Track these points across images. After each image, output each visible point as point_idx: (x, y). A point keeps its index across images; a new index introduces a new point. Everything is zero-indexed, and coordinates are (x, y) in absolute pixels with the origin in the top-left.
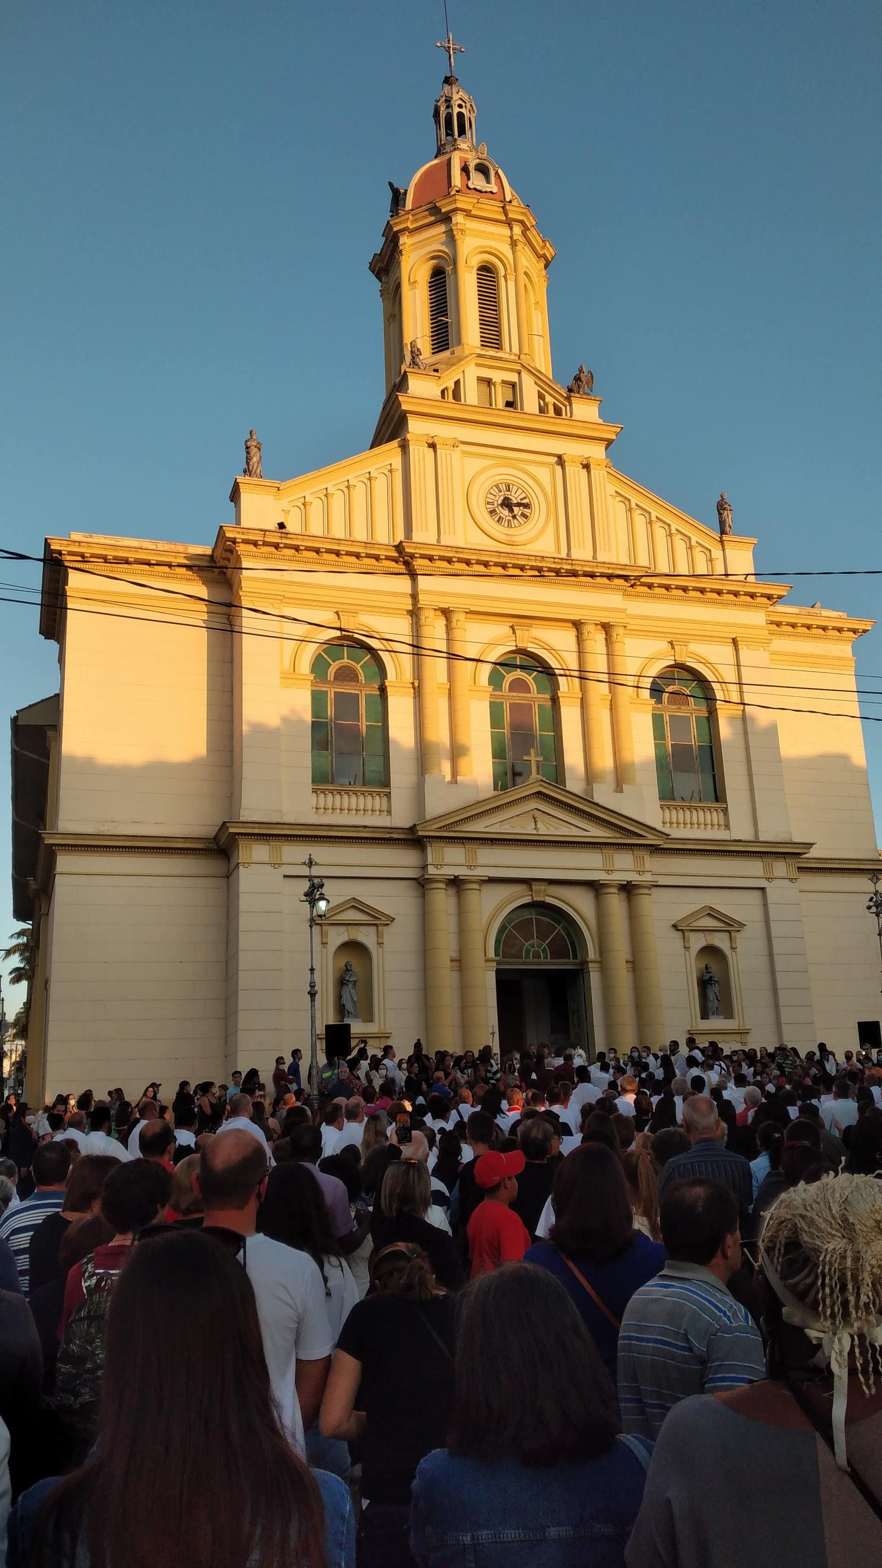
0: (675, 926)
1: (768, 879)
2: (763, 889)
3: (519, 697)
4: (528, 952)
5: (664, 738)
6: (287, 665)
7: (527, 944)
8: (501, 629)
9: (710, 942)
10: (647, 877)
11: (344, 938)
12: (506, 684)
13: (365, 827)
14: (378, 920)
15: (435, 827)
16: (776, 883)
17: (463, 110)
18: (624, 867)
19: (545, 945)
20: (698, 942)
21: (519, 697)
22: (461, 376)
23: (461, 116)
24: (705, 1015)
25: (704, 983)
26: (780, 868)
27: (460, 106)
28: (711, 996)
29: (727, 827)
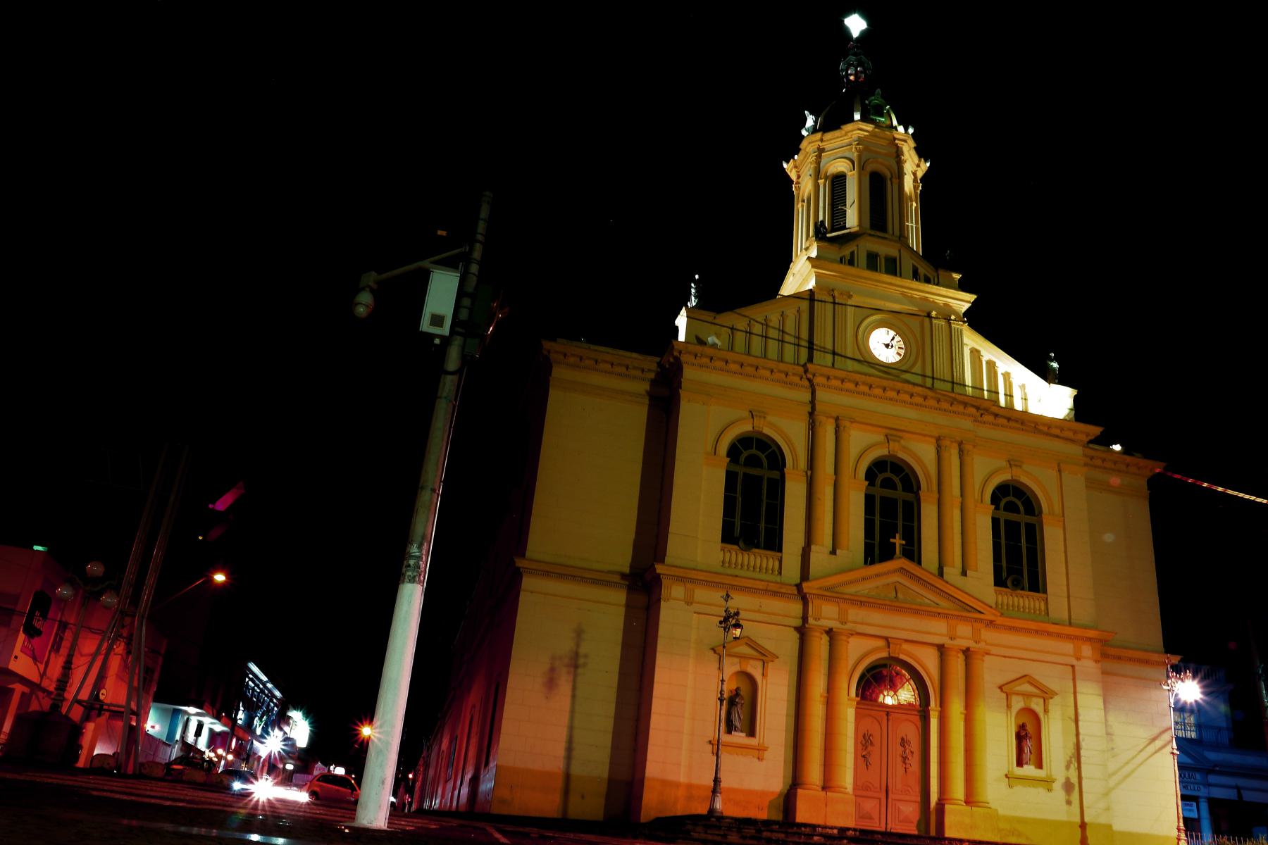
0: (1001, 688)
1: (1078, 659)
2: (1073, 666)
3: (888, 493)
6: (709, 448)
10: (982, 645)
11: (737, 668)
12: (878, 482)
14: (765, 657)
18: (964, 635)
20: (1018, 703)
21: (888, 493)
22: (855, 248)
24: (1020, 763)
25: (1021, 737)
28: (1027, 750)
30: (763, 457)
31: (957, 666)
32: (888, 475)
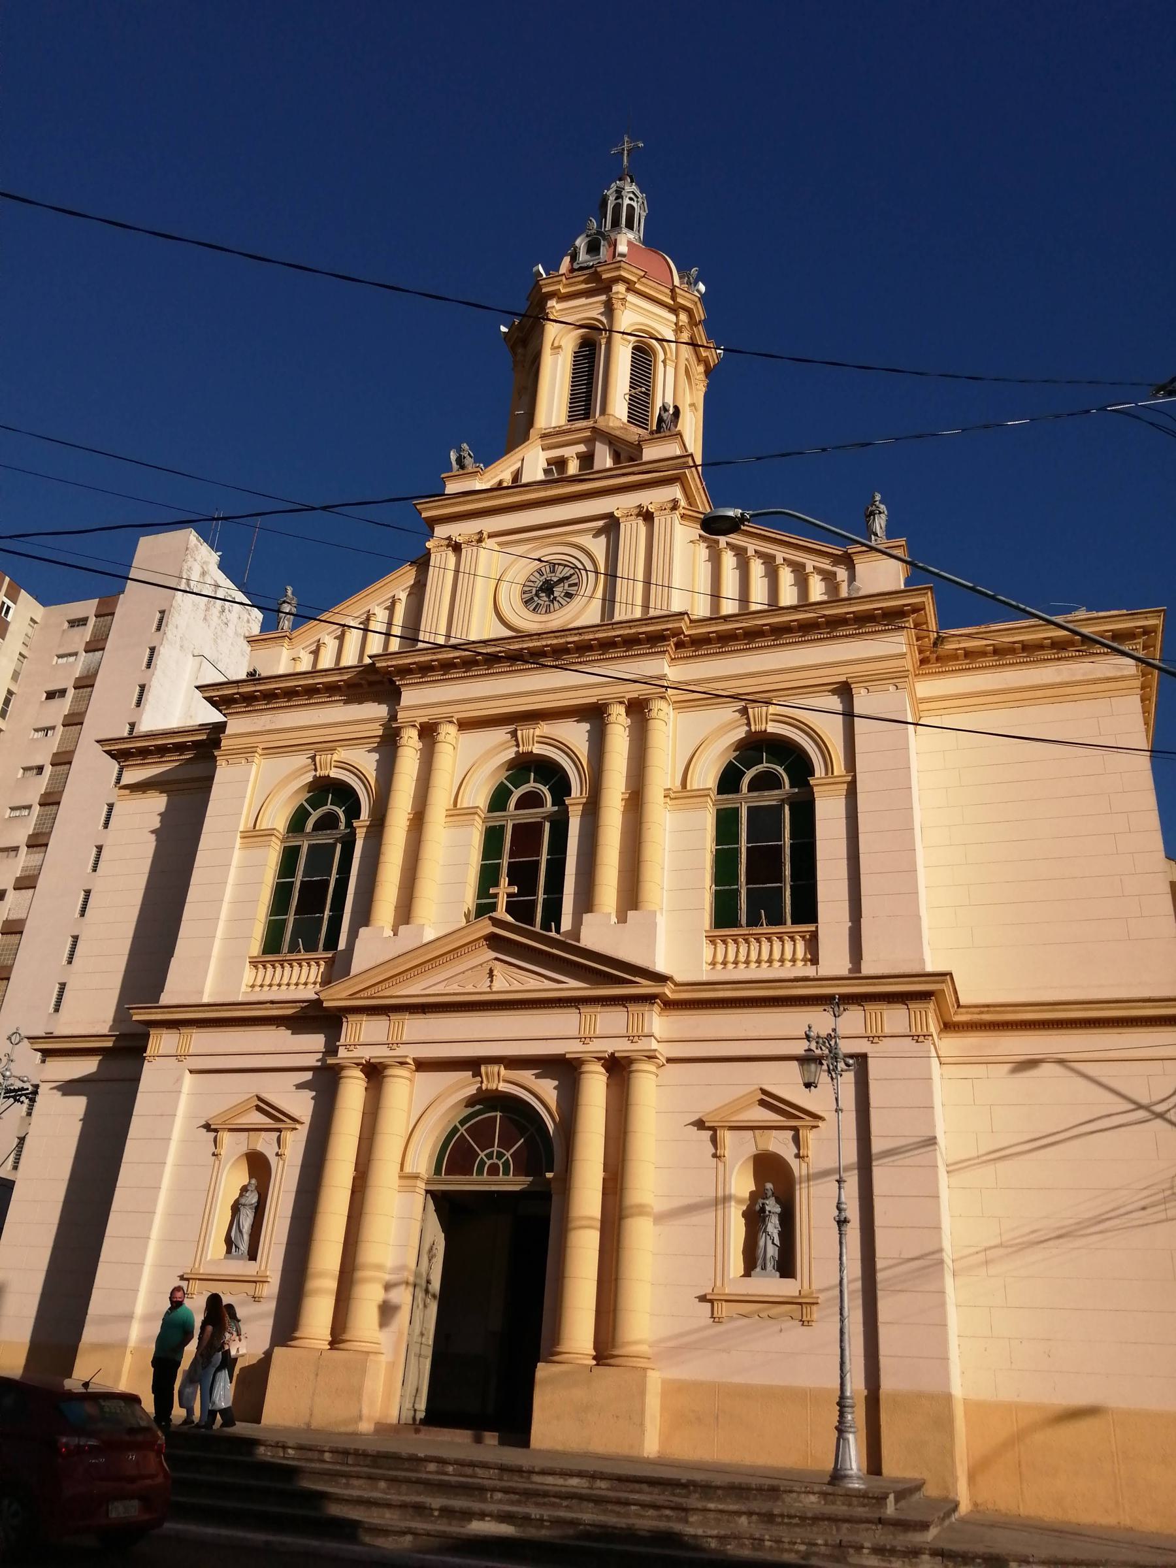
1: (872, 1039)
4: (482, 1163)
5: (736, 839)
7: (482, 1155)
8: (500, 735)
9: (762, 1146)
10: (642, 1045)
13: (272, 1002)
15: (344, 995)
16: (886, 1045)
17: (634, 204)
18: (607, 1030)
19: (508, 1155)
23: (630, 207)
26: (895, 1018)
27: (631, 199)
29: (815, 961)
30: (340, 812)
31: (595, 1087)
32: (531, 786)
